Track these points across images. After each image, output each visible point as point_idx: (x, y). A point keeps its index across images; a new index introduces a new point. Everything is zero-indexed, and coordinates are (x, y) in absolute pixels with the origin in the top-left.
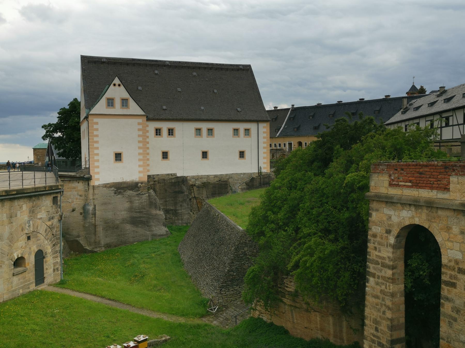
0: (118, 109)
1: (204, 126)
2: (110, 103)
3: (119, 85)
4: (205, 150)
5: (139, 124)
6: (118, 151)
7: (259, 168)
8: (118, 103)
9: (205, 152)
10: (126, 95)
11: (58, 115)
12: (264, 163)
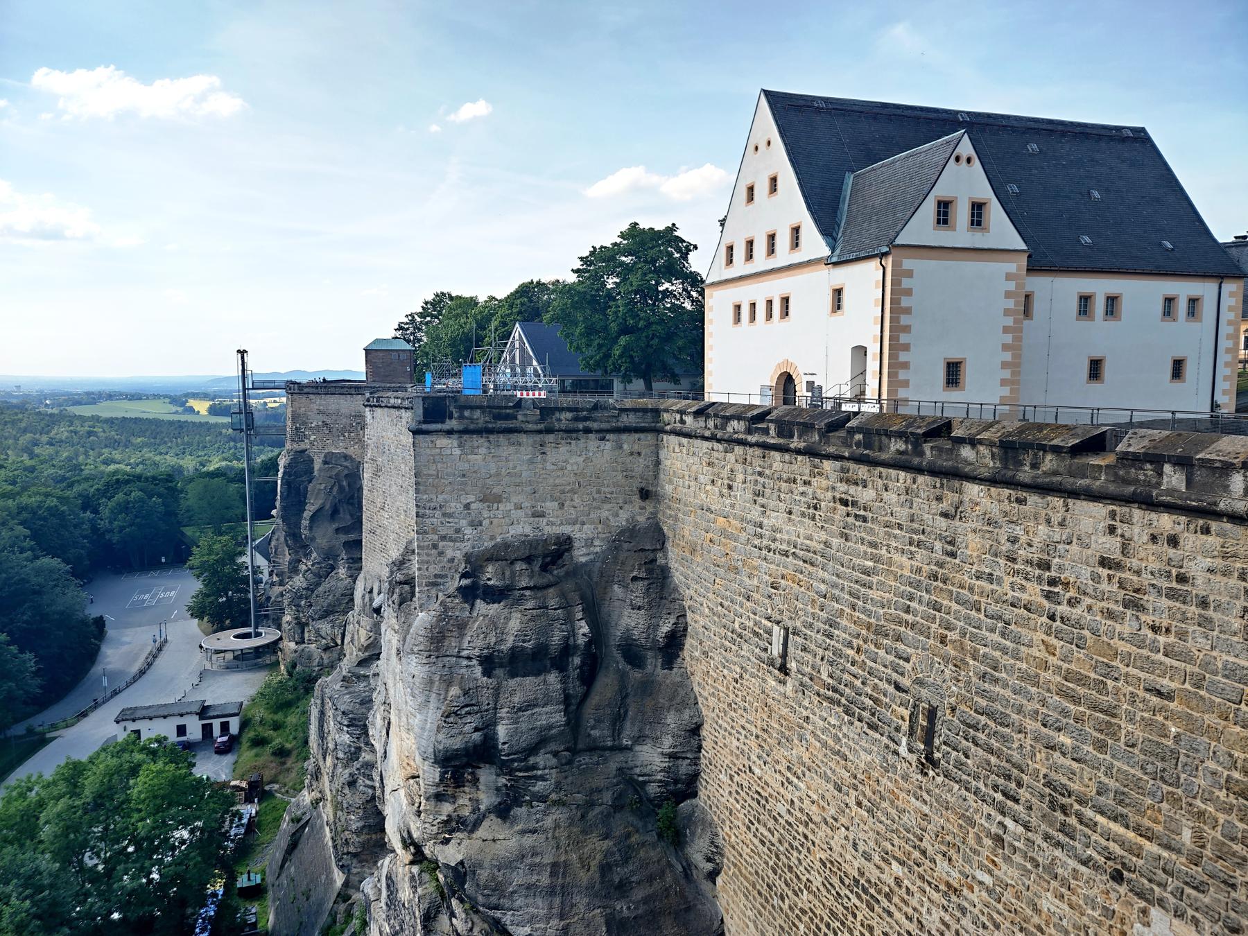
0: (961, 234)
1: (1100, 287)
2: (944, 211)
3: (969, 160)
4: (1097, 354)
5: (1009, 277)
6: (955, 355)
7: (1214, 406)
8: (962, 214)
9: (1097, 361)
10: (984, 191)
11: (578, 265)
12: (1225, 392)
